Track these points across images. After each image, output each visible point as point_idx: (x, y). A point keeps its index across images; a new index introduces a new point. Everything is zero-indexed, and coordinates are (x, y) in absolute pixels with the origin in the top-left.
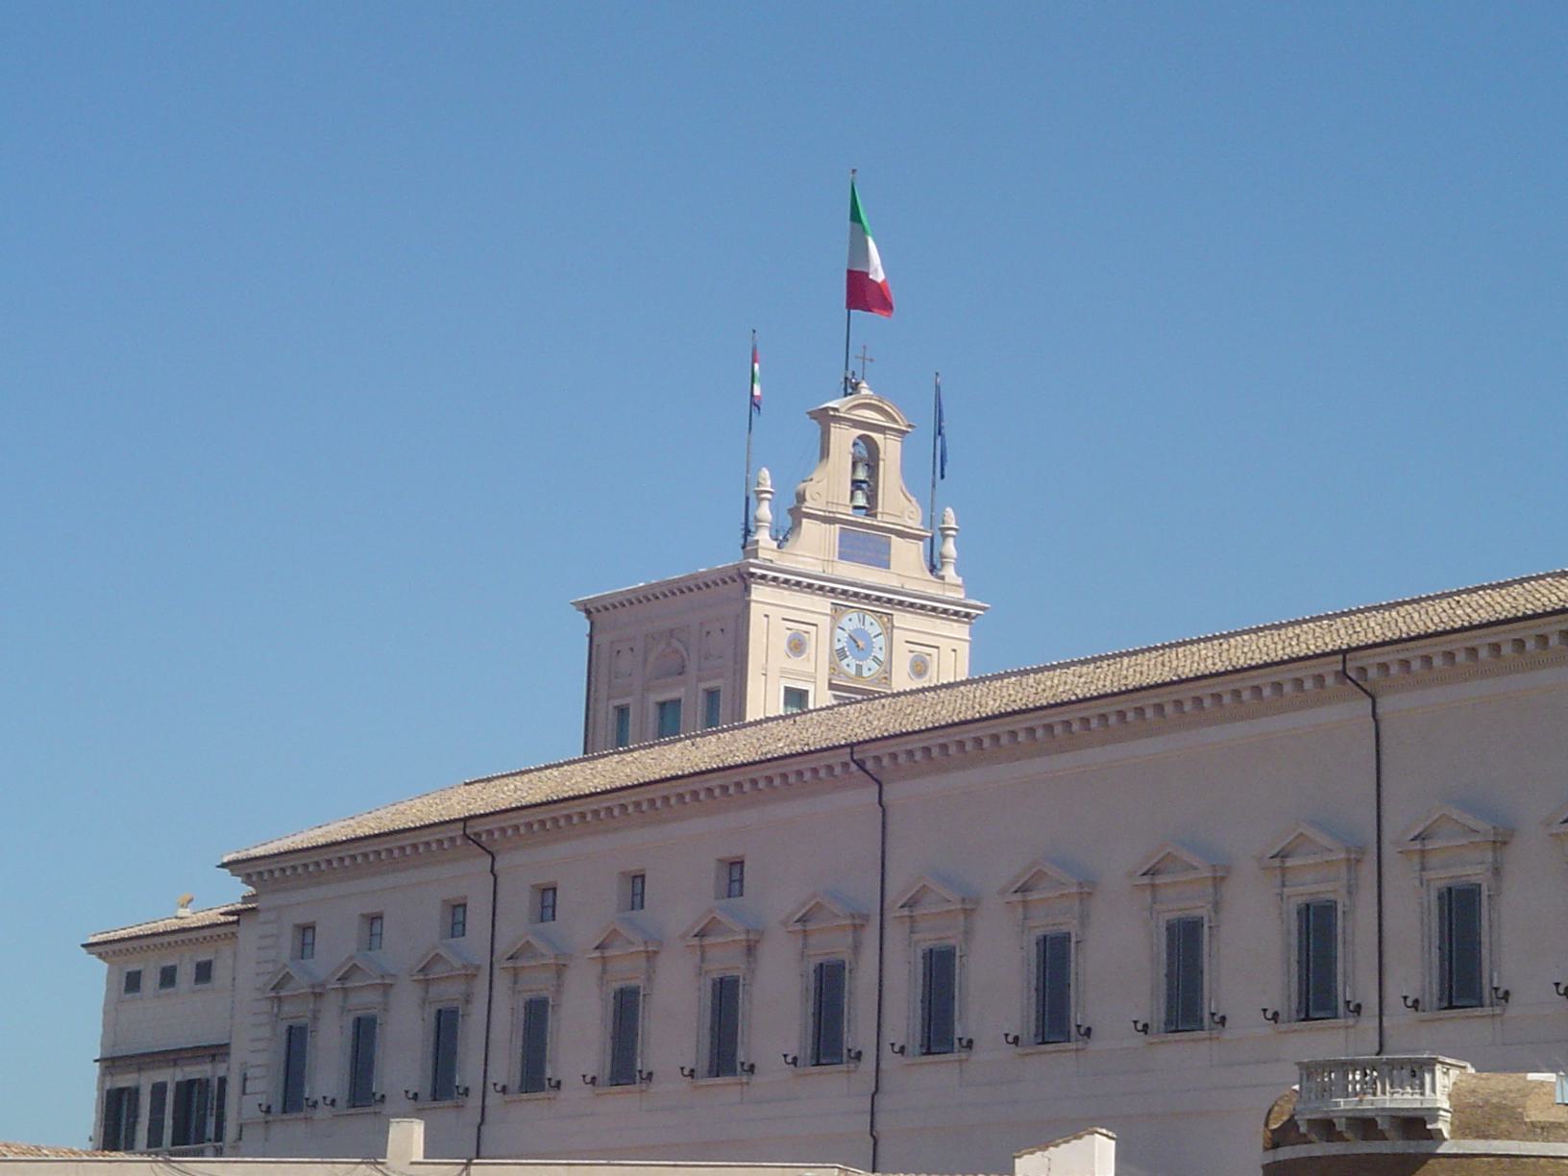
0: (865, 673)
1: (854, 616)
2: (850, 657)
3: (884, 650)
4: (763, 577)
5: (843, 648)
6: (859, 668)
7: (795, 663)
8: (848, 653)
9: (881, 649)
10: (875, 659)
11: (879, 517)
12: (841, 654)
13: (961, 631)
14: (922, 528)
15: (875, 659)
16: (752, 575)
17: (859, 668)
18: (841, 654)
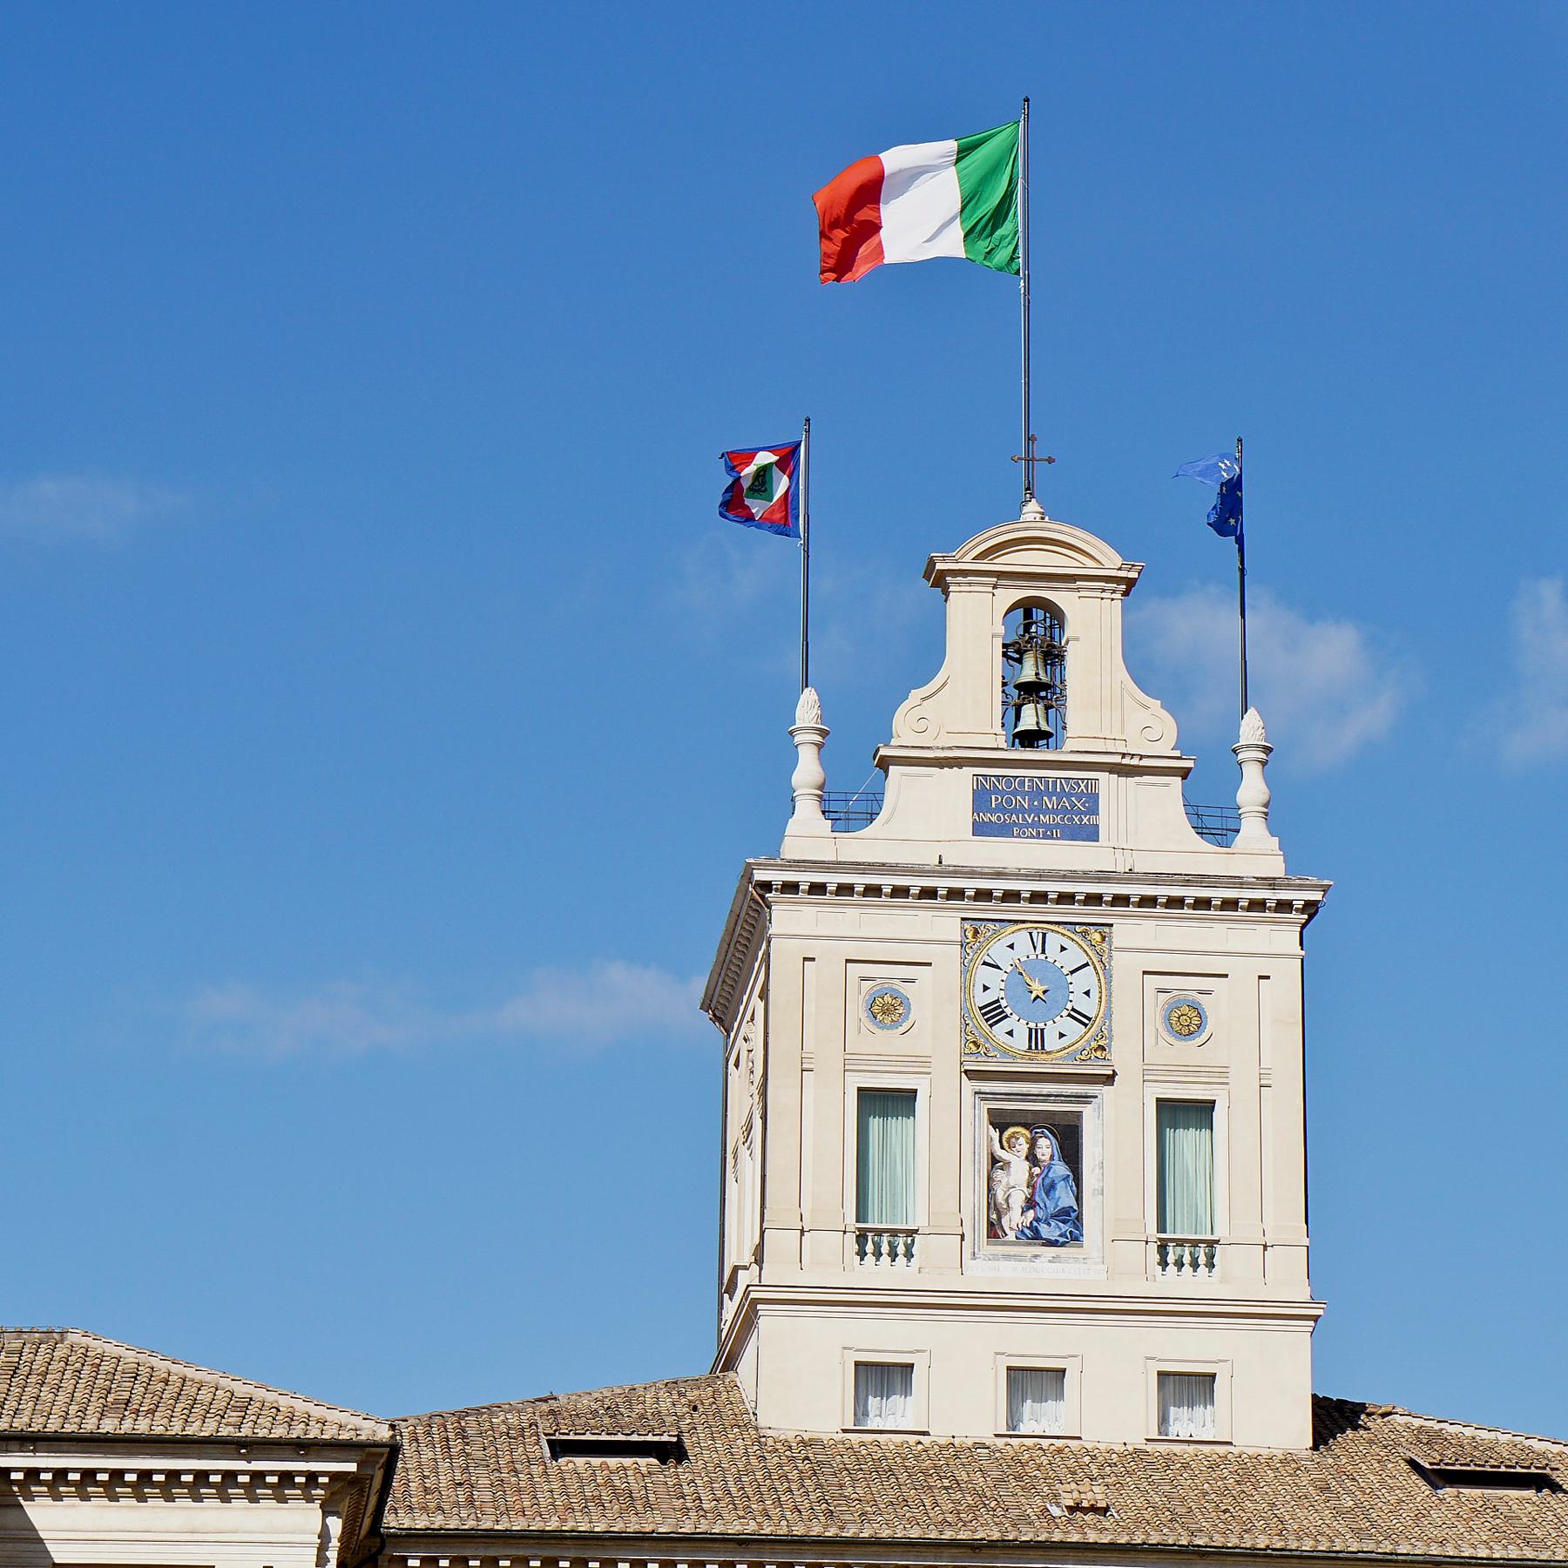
0: (1052, 1042)
1: (1021, 939)
2: (1015, 1017)
3: (1095, 994)
4: (791, 887)
5: (997, 1001)
6: (1036, 1038)
7: (887, 1042)
8: (1008, 1011)
9: (1087, 993)
10: (1077, 1016)
11: (1070, 745)
12: (994, 1013)
13: (1284, 937)
14: (1177, 753)
15: (1077, 1016)
16: (767, 886)
17: (1036, 1038)
18: (994, 1013)
